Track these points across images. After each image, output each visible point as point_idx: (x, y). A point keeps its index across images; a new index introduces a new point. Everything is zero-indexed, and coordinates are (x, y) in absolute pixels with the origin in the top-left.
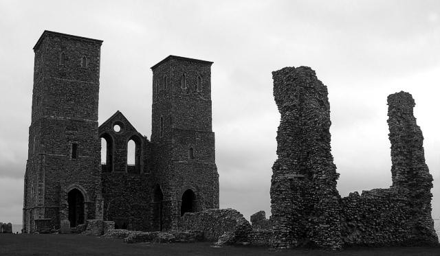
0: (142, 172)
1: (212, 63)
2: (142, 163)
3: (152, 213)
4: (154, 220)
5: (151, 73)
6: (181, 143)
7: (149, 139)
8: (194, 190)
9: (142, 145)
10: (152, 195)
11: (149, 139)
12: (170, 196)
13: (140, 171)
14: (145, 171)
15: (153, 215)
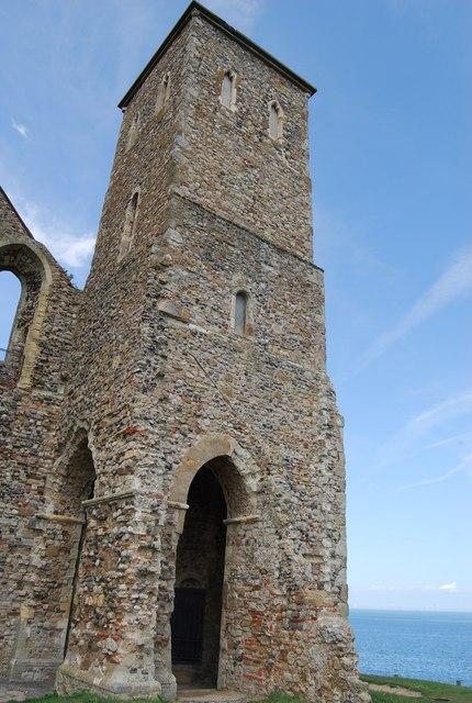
0: (25, 382)
1: (313, 91)
2: (32, 352)
3: (36, 560)
4: (38, 597)
5: (119, 114)
6: (208, 257)
7: (80, 282)
8: (244, 463)
9: (46, 287)
10: (54, 483)
11: (80, 282)
12: (130, 470)
13: (18, 374)
14: (37, 384)
15: (42, 570)
